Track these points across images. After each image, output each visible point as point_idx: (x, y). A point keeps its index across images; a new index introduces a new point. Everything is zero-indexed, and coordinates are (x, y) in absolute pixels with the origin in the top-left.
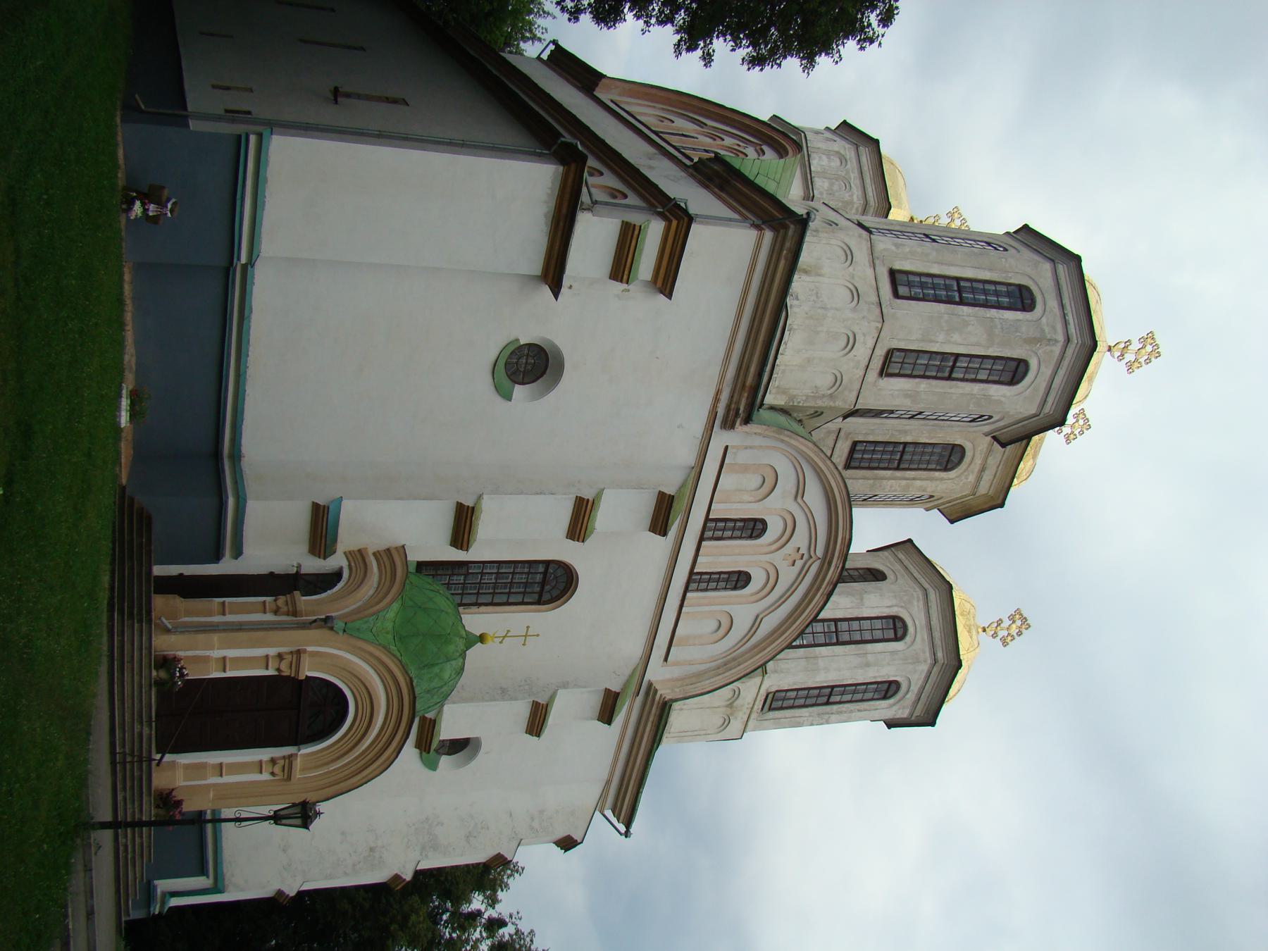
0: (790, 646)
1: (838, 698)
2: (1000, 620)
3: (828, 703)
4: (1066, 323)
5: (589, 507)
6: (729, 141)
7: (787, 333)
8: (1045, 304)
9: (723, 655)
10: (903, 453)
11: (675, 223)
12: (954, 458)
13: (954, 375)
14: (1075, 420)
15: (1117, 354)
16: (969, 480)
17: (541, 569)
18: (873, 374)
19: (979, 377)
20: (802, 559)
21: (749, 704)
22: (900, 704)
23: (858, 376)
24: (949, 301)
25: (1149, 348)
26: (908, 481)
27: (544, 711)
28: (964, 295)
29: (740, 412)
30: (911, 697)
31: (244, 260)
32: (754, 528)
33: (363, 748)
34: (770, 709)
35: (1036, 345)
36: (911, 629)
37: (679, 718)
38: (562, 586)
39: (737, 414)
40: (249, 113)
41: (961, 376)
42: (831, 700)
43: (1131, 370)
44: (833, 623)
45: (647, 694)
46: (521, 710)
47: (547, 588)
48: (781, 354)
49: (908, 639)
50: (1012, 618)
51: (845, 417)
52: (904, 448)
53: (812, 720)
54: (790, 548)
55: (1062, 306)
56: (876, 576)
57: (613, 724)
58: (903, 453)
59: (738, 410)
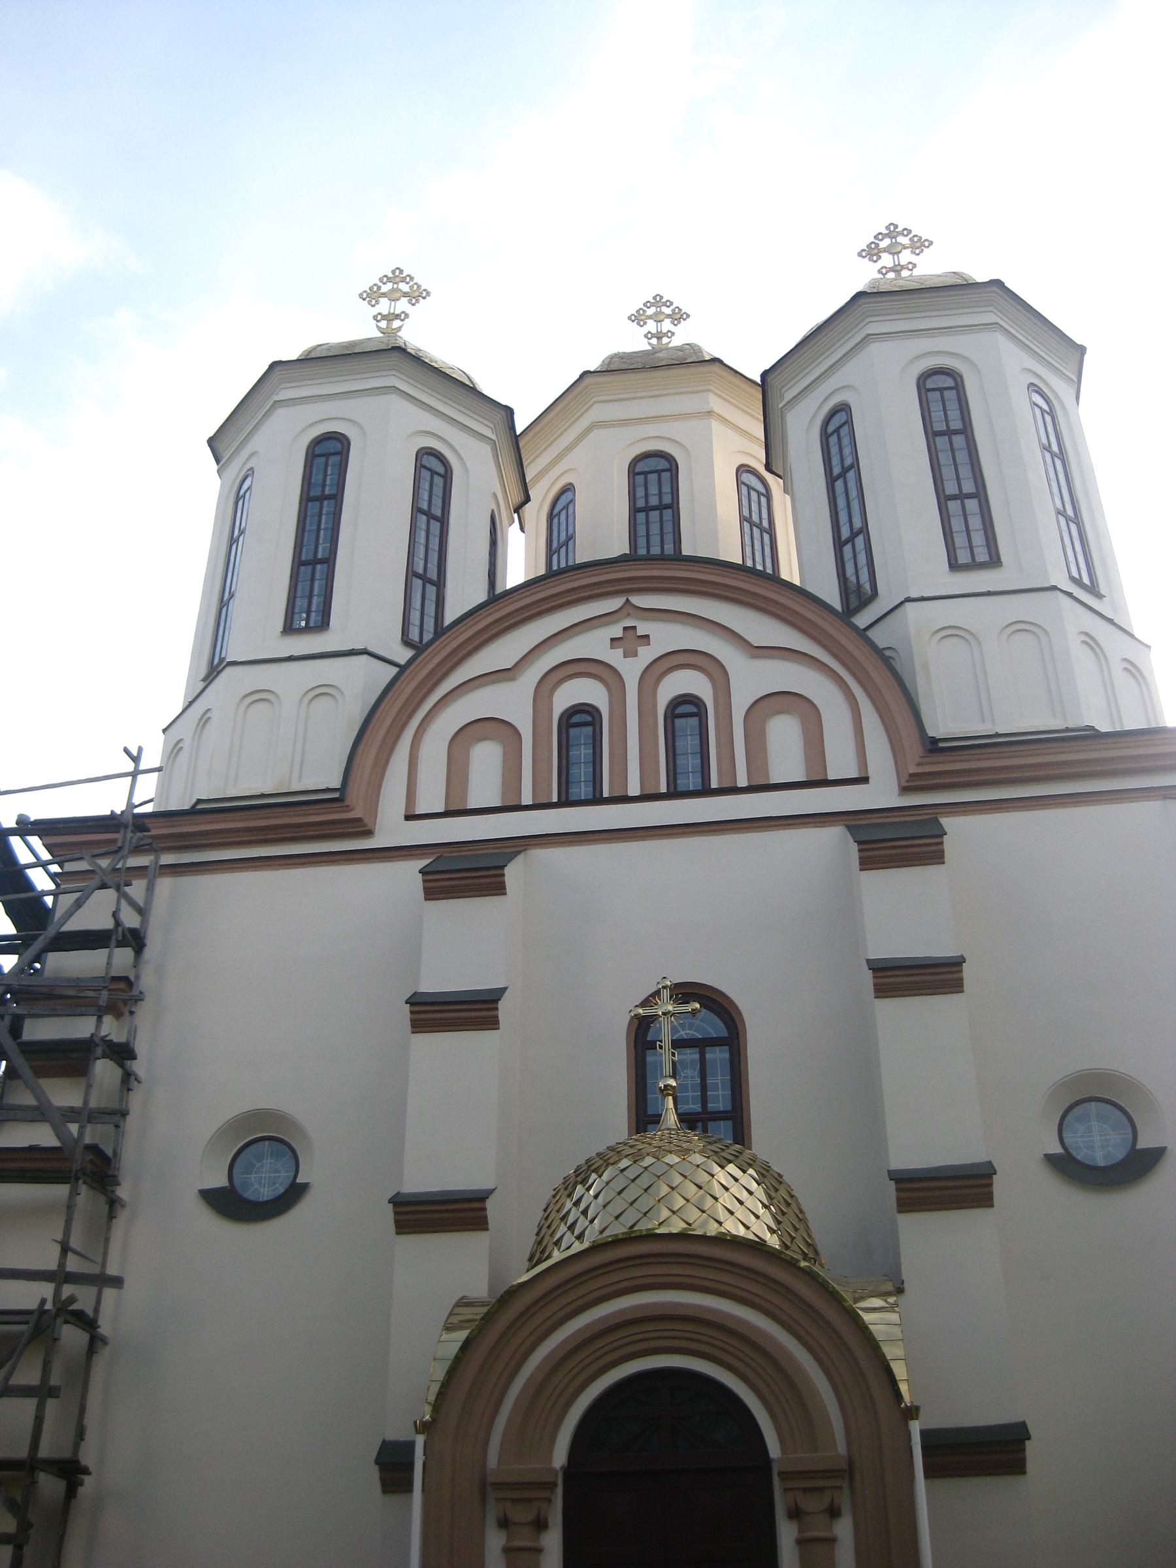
20: (635, 628)
54: (614, 657)
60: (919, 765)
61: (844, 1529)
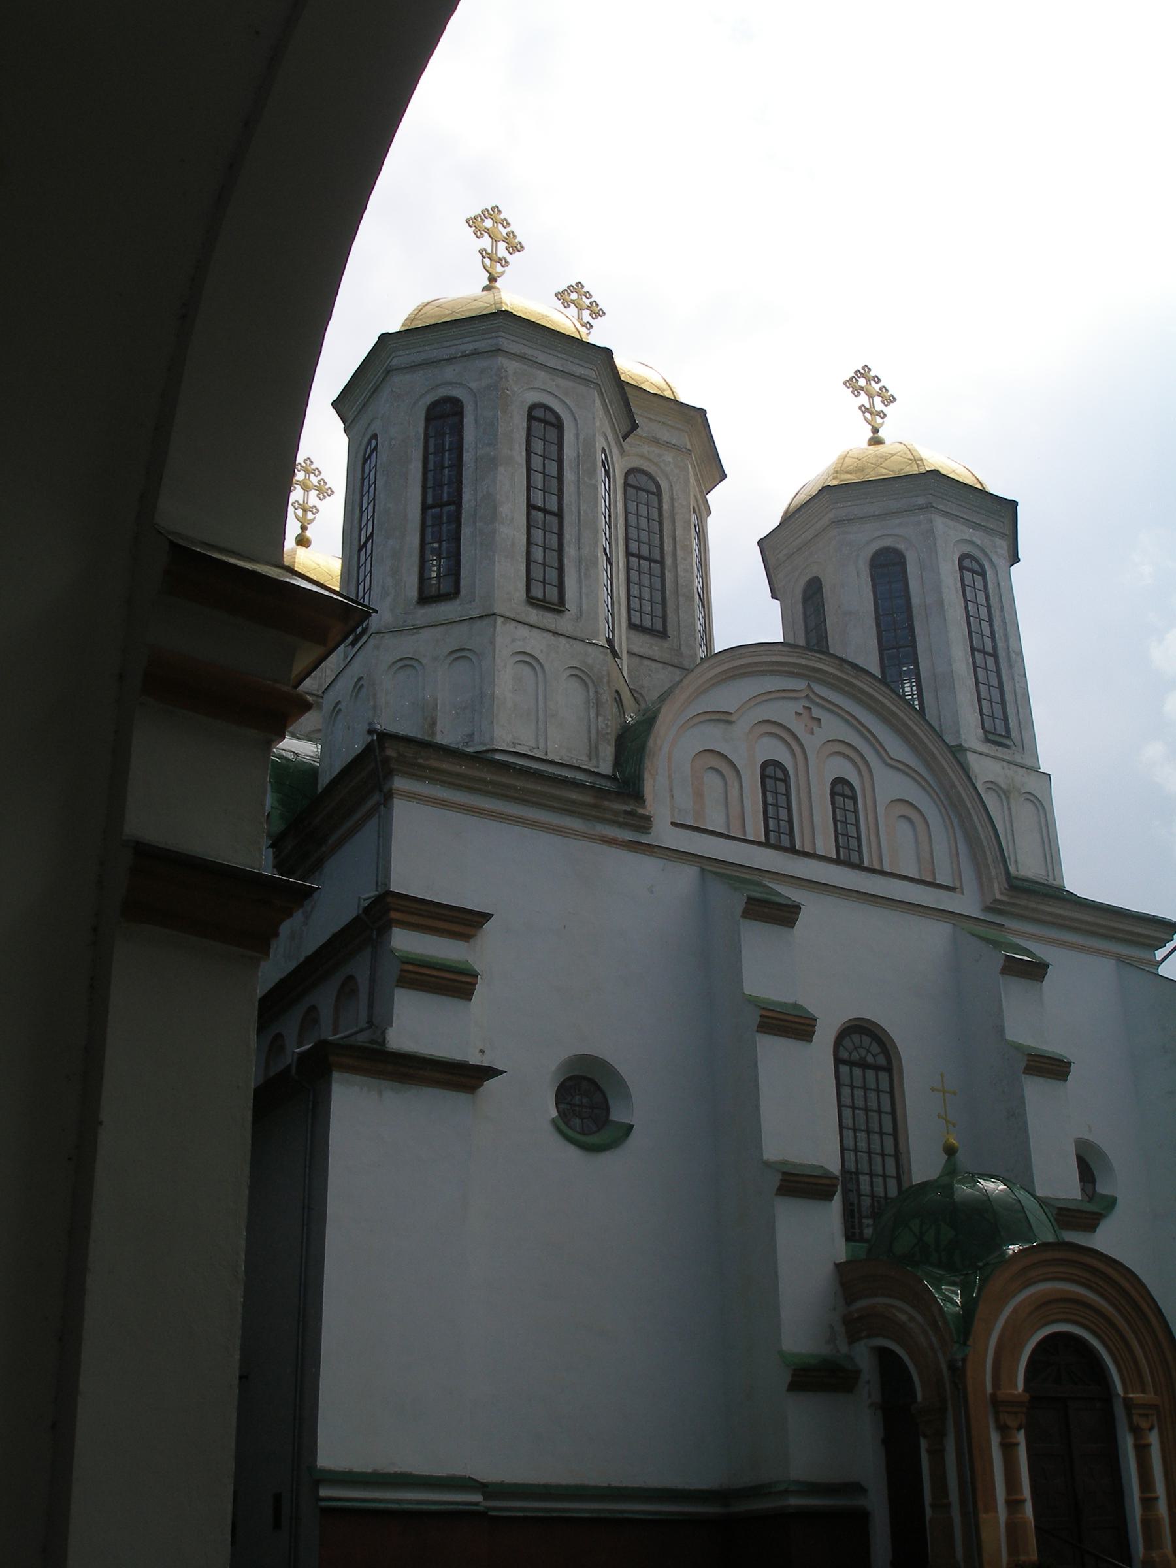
0: (922, 712)
1: (988, 641)
2: (860, 408)
3: (995, 655)
4: (475, 354)
5: (770, 1014)
7: (519, 750)
8: (451, 383)
9: (943, 810)
10: (640, 557)
11: (394, 915)
12: (643, 481)
13: (555, 508)
14: (572, 305)
15: (499, 268)
16: (672, 461)
17: (844, 1069)
18: (563, 623)
19: (555, 473)
20: (811, 708)
21: (1003, 768)
22: (988, 551)
23: (568, 646)
24: (457, 519)
26: (678, 547)
27: (1037, 1059)
28: (445, 499)
29: (629, 809)
30: (978, 537)
31: (477, 1498)
33: (1111, 1309)
34: (1008, 736)
35: (509, 395)
36: (888, 542)
37: (1028, 866)
38: (866, 1040)
39: (631, 814)
40: (278, 1498)
41: (555, 498)
42: (989, 649)
43: (519, 246)
44: (885, 652)
45: (1000, 912)
46: (1035, 1090)
47: (870, 1059)
48: (546, 754)
49: (901, 546)
50: (856, 391)
51: (615, 654)
52: (634, 555)
53: (1019, 675)
54: (798, 727)
55: (451, 360)
56: (813, 594)
57: (1047, 959)
58: (640, 557)
59: (626, 812)
60: (1001, 894)
61: (1154, 1438)
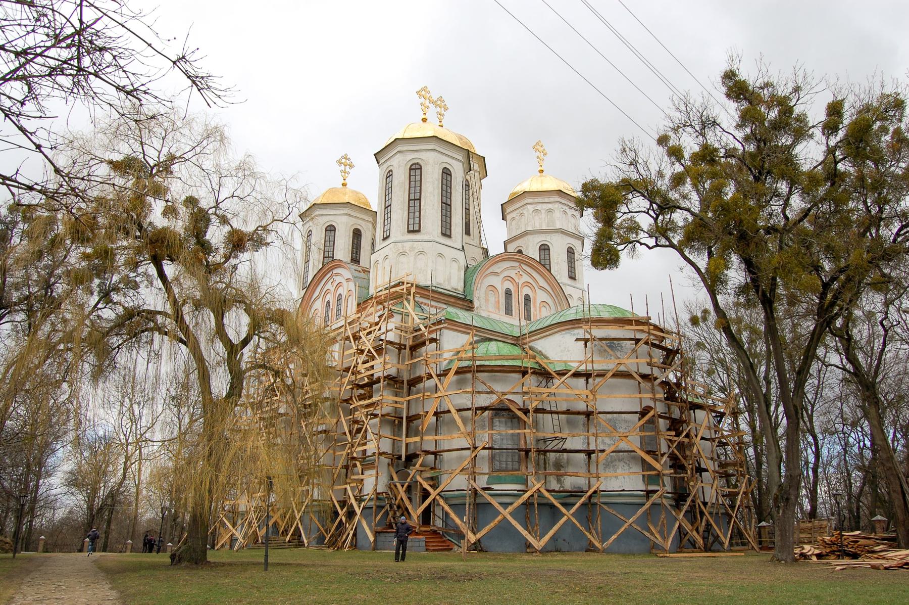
0: (549, 271)
6: (329, 286)
25: (423, 93)
32: (508, 293)
